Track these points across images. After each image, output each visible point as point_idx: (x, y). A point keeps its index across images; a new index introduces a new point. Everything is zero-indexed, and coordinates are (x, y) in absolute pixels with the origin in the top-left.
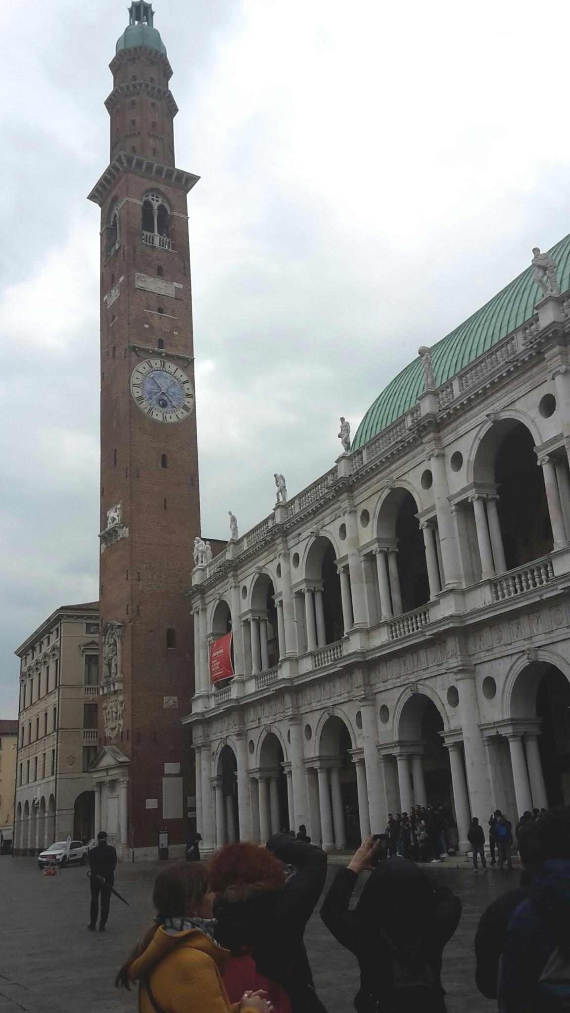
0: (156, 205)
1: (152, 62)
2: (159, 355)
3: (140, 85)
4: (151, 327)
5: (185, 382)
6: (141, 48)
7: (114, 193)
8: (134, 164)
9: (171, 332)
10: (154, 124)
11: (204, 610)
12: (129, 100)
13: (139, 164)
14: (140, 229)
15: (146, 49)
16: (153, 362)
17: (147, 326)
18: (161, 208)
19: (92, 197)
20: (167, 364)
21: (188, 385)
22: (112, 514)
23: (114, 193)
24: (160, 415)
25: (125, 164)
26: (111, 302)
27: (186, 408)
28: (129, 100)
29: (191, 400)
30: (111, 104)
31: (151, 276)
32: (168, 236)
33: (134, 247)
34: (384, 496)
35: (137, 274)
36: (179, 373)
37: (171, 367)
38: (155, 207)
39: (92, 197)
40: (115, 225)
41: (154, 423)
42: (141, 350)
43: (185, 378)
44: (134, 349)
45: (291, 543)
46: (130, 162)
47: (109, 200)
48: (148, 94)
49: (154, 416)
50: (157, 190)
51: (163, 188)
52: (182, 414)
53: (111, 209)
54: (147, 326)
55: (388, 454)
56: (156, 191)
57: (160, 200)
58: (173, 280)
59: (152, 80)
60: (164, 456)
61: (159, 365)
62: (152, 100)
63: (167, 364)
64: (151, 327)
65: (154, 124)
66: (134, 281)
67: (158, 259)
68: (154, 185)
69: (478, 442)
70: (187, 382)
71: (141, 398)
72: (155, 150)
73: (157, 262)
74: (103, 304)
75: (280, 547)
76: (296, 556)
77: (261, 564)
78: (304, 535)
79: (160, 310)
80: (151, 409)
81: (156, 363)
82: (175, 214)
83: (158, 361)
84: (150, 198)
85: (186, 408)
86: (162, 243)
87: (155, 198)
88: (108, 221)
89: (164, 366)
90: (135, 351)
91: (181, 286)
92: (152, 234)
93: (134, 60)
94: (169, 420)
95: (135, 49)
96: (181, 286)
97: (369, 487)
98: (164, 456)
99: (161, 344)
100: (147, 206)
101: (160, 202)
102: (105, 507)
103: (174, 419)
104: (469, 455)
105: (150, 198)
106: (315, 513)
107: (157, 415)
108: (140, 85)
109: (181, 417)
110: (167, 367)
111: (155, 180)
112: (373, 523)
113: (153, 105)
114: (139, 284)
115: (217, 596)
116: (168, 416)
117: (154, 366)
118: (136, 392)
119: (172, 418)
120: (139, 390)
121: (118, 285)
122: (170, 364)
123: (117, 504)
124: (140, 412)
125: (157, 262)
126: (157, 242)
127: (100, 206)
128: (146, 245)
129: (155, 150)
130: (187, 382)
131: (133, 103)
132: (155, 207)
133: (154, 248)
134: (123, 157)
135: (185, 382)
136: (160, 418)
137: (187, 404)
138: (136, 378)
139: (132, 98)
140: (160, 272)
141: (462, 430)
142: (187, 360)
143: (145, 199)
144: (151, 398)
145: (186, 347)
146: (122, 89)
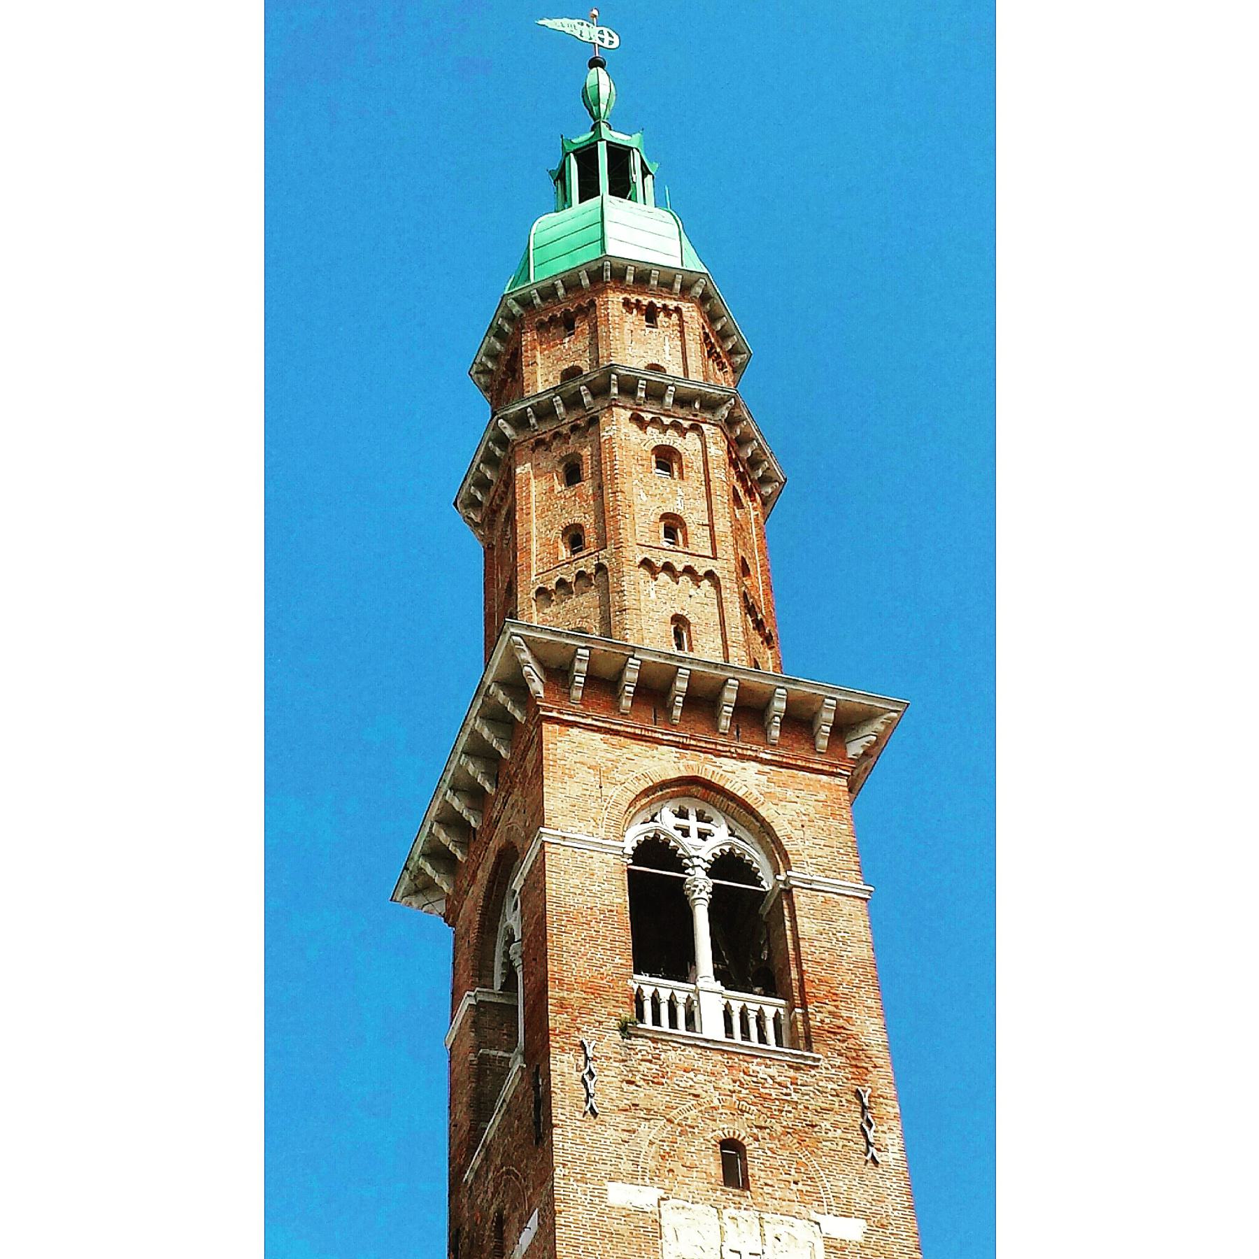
1: (651, 314)
18: (727, 865)
72: (680, 622)
87: (693, 824)
92: (682, 992)
95: (571, 282)
101: (720, 835)
108: (600, 391)
126: (712, 1026)
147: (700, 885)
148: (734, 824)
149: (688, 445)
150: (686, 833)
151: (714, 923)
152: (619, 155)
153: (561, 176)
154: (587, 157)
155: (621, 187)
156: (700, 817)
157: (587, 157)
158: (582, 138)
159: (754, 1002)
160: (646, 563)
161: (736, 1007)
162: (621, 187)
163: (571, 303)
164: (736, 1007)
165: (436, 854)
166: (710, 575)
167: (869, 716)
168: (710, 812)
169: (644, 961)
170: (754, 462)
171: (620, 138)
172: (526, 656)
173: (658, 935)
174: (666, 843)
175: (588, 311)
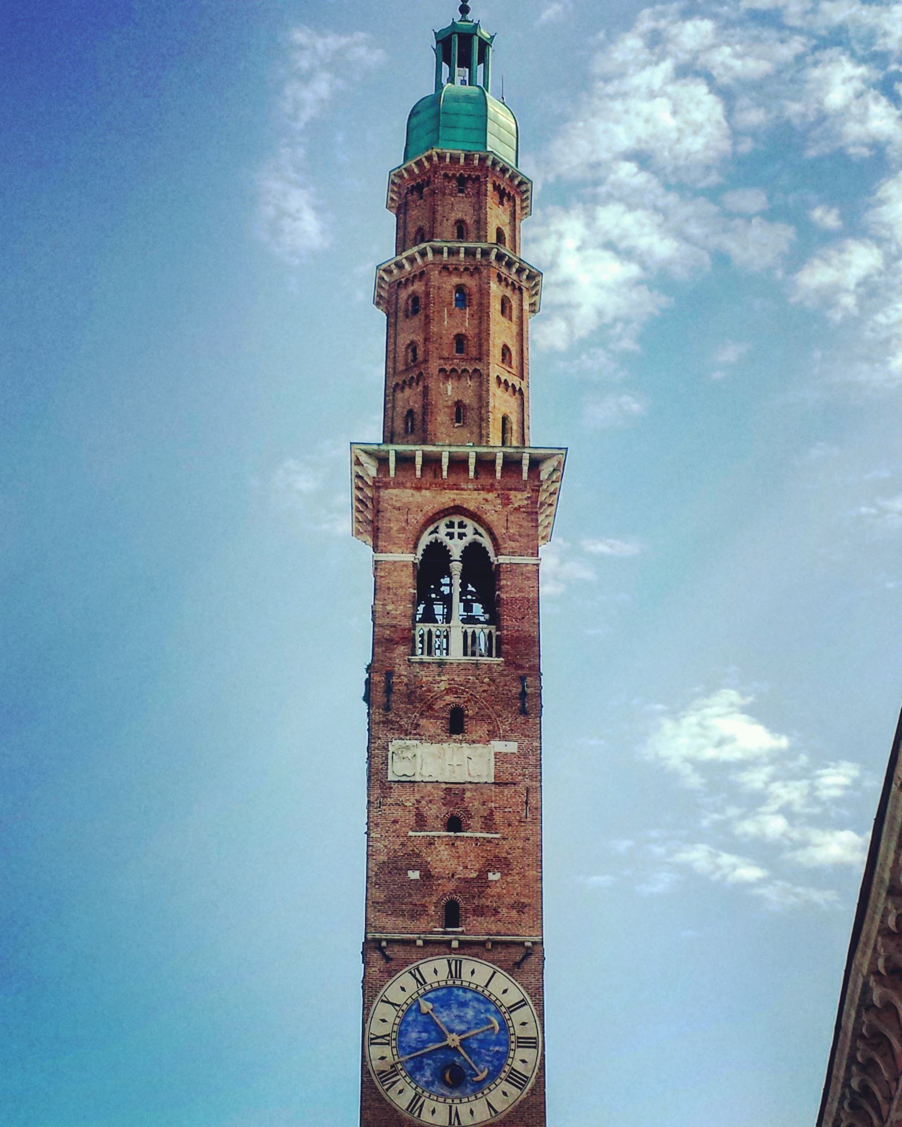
0: (456, 548)
4: (427, 875)
5: (512, 1009)
8: (392, 465)
12: (404, 295)
16: (426, 969)
17: (414, 875)
18: (474, 552)
20: (467, 966)
21: (525, 1014)
25: (373, 472)
27: (516, 1079)
28: (404, 295)
31: (432, 739)
33: (389, 674)
35: (395, 745)
43: (515, 994)
50: (458, 510)
54: (414, 875)
57: (469, 531)
58: (493, 734)
61: (443, 973)
62: (455, 280)
63: (467, 966)
64: (427, 875)
68: (447, 498)
70: (522, 1003)
73: (449, 698)
79: (454, 824)
82: (502, 559)
83: (441, 964)
84: (443, 530)
85: (516, 1079)
86: (469, 644)
87: (456, 530)
90: (381, 949)
91: (511, 747)
96: (511, 747)
101: (470, 537)
108: (423, 254)
110: (466, 975)
111: (456, 487)
113: (460, 289)
114: (397, 769)
117: (430, 978)
122: (477, 967)
124: (390, 1109)
125: (449, 698)
128: (421, 663)
130: (522, 1003)
131: (415, 299)
134: (363, 458)
135: (512, 1009)
139: (411, 289)
140: (456, 724)
143: (426, 539)
145: (521, 908)
147: (456, 567)
148: (477, 526)
150: (451, 535)
152: (466, 38)
156: (462, 525)
160: (442, 370)
161: (470, 632)
164: (470, 632)
166: (476, 370)
168: (467, 521)
170: (520, 271)
172: (363, 458)
174: (441, 543)
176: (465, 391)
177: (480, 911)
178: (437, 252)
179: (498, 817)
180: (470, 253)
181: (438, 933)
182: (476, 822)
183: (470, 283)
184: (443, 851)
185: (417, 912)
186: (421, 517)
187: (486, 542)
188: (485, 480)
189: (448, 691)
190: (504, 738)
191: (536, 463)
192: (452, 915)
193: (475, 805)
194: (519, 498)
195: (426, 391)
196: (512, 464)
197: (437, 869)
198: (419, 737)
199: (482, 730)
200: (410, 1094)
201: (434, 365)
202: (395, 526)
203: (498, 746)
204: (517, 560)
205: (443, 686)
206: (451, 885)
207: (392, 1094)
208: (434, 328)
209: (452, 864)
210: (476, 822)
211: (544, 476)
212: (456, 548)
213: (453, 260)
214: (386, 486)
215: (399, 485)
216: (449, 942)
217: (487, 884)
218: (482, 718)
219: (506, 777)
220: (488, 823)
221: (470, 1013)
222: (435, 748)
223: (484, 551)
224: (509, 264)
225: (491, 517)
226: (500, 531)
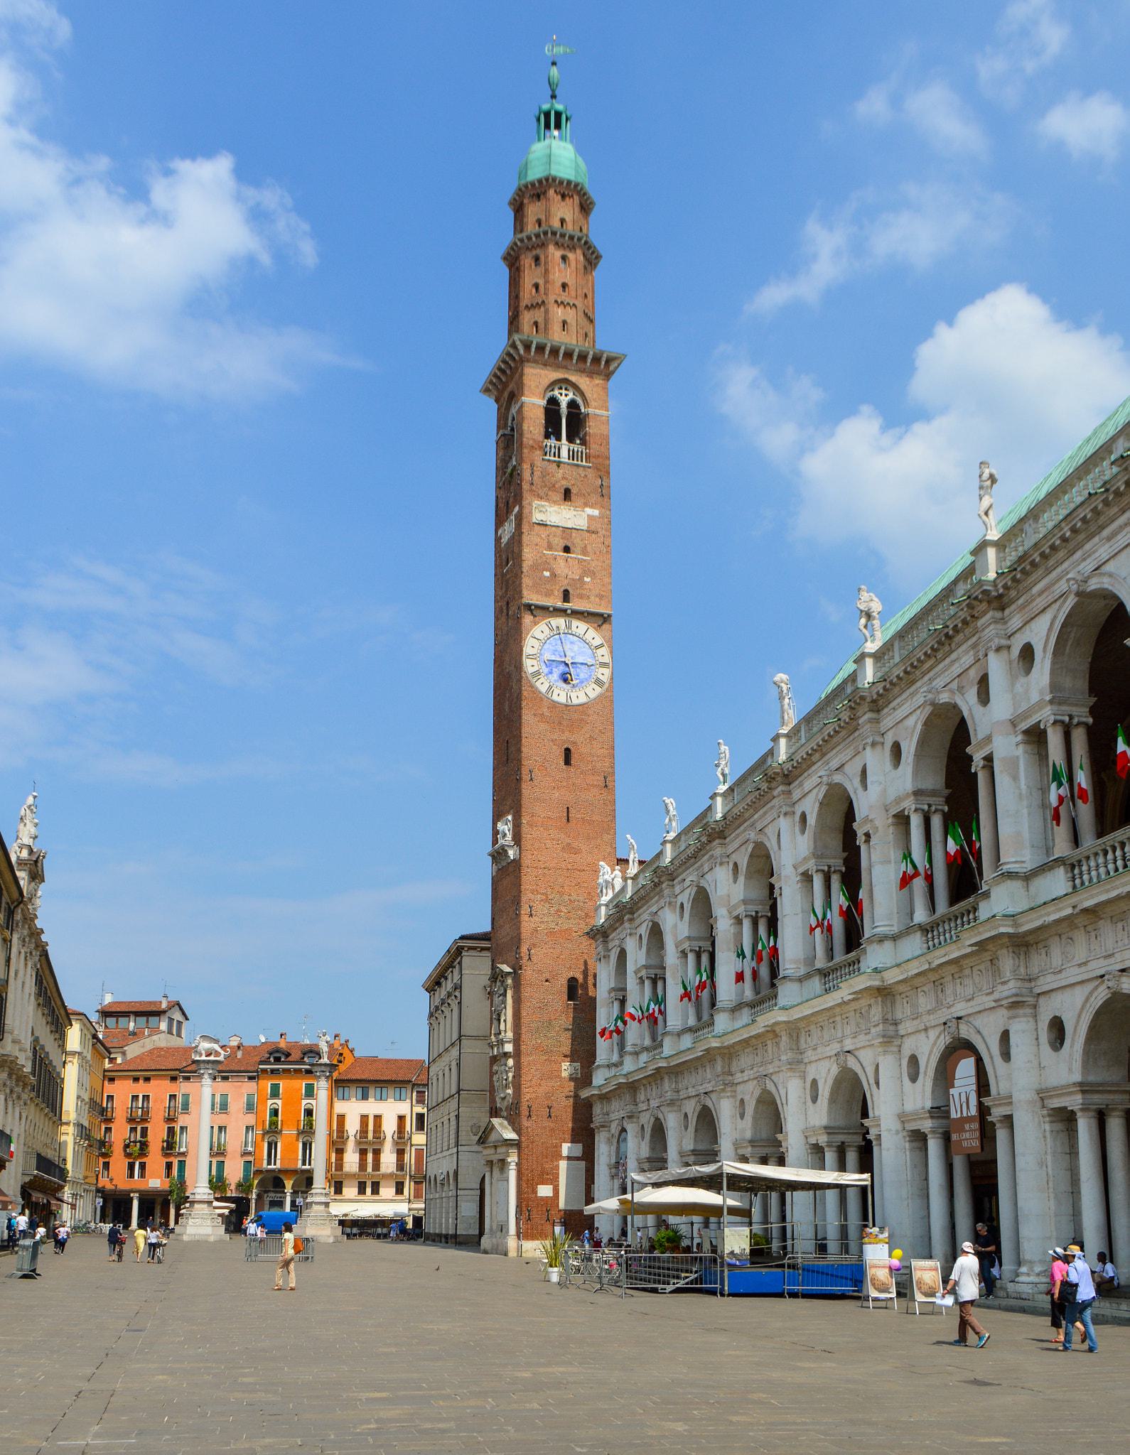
0: (564, 402)
1: (563, 196)
2: (562, 612)
3: (545, 233)
4: (554, 575)
5: (597, 647)
6: (547, 179)
7: (509, 389)
9: (581, 579)
10: (564, 286)
11: (606, 957)
13: (541, 348)
14: (541, 438)
15: (554, 179)
17: (547, 574)
18: (572, 404)
19: (486, 390)
22: (501, 826)
23: (509, 389)
24: (563, 695)
25: (522, 352)
26: (504, 540)
27: (599, 682)
29: (607, 672)
30: (512, 260)
31: (555, 502)
32: (584, 443)
34: (750, 850)
35: (536, 503)
36: (592, 633)
37: (579, 626)
38: (564, 405)
39: (486, 390)
40: (512, 429)
41: (554, 705)
42: (537, 607)
44: (529, 607)
45: (677, 889)
46: (527, 347)
47: (506, 394)
48: (557, 244)
49: (555, 698)
50: (566, 381)
51: (573, 378)
52: (593, 691)
53: (508, 408)
54: (547, 574)
55: (748, 801)
56: (564, 383)
58: (586, 505)
59: (562, 221)
60: (568, 751)
63: (575, 623)
64: (554, 575)
65: (564, 286)
66: (531, 513)
67: (564, 478)
69: (817, 805)
70: (602, 646)
71: (537, 673)
72: (564, 323)
74: (498, 539)
75: (666, 892)
76: (682, 905)
77: (654, 909)
78: (687, 883)
79: (567, 549)
80: (550, 687)
81: (560, 622)
82: (590, 410)
84: (556, 392)
85: (599, 682)
86: (572, 455)
87: (564, 392)
88: (505, 426)
89: (570, 627)
90: (531, 611)
91: (596, 512)
93: (538, 197)
94: (575, 701)
95: (540, 181)
96: (596, 512)
97: (738, 835)
98: (568, 751)
99: (566, 596)
100: (553, 402)
101: (571, 396)
102: (497, 816)
103: (583, 699)
104: (812, 820)
105: (556, 392)
106: (695, 856)
107: (561, 695)
108: (545, 233)
109: (593, 695)
112: (741, 879)
114: (537, 517)
115: (617, 942)
116: (573, 695)
118: (529, 666)
119: (579, 697)
120: (534, 662)
121: (513, 518)
123: (508, 813)
124: (536, 691)
127: (497, 401)
129: (564, 323)
130: (602, 646)
132: (564, 405)
133: (559, 464)
134: (518, 343)
135: (597, 647)
136: (562, 699)
137: (600, 677)
138: (530, 646)
139: (534, 253)
140: (567, 495)
141: (808, 785)
142: (601, 615)
143: (549, 394)
144: (551, 673)
145: (601, 597)
146: (521, 240)
149: (571, 256)
151: (568, 422)
152: (558, 115)
153: (538, 120)
154: (547, 115)
155: (558, 126)
157: (547, 115)
158: (546, 107)
159: (576, 447)
162: (558, 126)
163: (538, 190)
165: (491, 382)
167: (616, 358)
169: (547, 436)
171: (560, 107)
173: (552, 428)
175: (545, 193)
176: (570, 315)
177: (581, 597)
178: (554, 233)
179: (589, 548)
180: (571, 238)
181: (559, 604)
182: (578, 550)
183: (571, 256)
184: (562, 563)
185: (549, 594)
186: (546, 382)
187: (579, 400)
188: (581, 365)
189: (564, 478)
190: (591, 507)
191: (608, 361)
192: (566, 596)
193: (577, 541)
194: (598, 381)
195: (547, 312)
196: (597, 360)
197: (558, 572)
198: (548, 500)
199: (581, 501)
200: (546, 685)
201: (552, 298)
202: (533, 384)
203: (589, 511)
204: (597, 412)
205: (560, 475)
206: (566, 582)
207: (538, 684)
208: (551, 277)
209: (566, 571)
210: (578, 550)
211: (611, 368)
212: (564, 402)
213: (561, 240)
214: (528, 361)
215: (536, 362)
216: (565, 611)
217: (584, 583)
218: (579, 494)
219: (593, 528)
220: (584, 552)
221: (576, 648)
222: (556, 508)
223: (578, 407)
224: (589, 248)
225: (583, 387)
226: (588, 395)
